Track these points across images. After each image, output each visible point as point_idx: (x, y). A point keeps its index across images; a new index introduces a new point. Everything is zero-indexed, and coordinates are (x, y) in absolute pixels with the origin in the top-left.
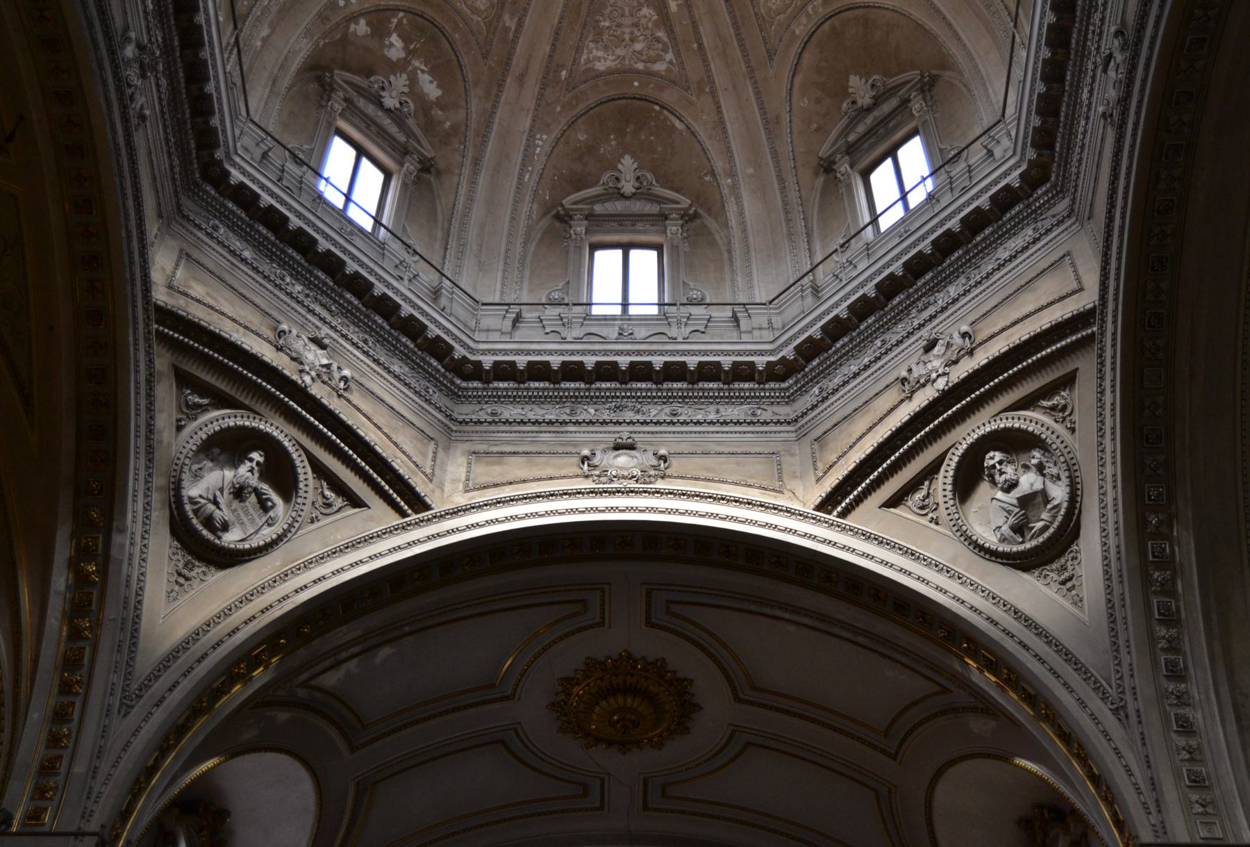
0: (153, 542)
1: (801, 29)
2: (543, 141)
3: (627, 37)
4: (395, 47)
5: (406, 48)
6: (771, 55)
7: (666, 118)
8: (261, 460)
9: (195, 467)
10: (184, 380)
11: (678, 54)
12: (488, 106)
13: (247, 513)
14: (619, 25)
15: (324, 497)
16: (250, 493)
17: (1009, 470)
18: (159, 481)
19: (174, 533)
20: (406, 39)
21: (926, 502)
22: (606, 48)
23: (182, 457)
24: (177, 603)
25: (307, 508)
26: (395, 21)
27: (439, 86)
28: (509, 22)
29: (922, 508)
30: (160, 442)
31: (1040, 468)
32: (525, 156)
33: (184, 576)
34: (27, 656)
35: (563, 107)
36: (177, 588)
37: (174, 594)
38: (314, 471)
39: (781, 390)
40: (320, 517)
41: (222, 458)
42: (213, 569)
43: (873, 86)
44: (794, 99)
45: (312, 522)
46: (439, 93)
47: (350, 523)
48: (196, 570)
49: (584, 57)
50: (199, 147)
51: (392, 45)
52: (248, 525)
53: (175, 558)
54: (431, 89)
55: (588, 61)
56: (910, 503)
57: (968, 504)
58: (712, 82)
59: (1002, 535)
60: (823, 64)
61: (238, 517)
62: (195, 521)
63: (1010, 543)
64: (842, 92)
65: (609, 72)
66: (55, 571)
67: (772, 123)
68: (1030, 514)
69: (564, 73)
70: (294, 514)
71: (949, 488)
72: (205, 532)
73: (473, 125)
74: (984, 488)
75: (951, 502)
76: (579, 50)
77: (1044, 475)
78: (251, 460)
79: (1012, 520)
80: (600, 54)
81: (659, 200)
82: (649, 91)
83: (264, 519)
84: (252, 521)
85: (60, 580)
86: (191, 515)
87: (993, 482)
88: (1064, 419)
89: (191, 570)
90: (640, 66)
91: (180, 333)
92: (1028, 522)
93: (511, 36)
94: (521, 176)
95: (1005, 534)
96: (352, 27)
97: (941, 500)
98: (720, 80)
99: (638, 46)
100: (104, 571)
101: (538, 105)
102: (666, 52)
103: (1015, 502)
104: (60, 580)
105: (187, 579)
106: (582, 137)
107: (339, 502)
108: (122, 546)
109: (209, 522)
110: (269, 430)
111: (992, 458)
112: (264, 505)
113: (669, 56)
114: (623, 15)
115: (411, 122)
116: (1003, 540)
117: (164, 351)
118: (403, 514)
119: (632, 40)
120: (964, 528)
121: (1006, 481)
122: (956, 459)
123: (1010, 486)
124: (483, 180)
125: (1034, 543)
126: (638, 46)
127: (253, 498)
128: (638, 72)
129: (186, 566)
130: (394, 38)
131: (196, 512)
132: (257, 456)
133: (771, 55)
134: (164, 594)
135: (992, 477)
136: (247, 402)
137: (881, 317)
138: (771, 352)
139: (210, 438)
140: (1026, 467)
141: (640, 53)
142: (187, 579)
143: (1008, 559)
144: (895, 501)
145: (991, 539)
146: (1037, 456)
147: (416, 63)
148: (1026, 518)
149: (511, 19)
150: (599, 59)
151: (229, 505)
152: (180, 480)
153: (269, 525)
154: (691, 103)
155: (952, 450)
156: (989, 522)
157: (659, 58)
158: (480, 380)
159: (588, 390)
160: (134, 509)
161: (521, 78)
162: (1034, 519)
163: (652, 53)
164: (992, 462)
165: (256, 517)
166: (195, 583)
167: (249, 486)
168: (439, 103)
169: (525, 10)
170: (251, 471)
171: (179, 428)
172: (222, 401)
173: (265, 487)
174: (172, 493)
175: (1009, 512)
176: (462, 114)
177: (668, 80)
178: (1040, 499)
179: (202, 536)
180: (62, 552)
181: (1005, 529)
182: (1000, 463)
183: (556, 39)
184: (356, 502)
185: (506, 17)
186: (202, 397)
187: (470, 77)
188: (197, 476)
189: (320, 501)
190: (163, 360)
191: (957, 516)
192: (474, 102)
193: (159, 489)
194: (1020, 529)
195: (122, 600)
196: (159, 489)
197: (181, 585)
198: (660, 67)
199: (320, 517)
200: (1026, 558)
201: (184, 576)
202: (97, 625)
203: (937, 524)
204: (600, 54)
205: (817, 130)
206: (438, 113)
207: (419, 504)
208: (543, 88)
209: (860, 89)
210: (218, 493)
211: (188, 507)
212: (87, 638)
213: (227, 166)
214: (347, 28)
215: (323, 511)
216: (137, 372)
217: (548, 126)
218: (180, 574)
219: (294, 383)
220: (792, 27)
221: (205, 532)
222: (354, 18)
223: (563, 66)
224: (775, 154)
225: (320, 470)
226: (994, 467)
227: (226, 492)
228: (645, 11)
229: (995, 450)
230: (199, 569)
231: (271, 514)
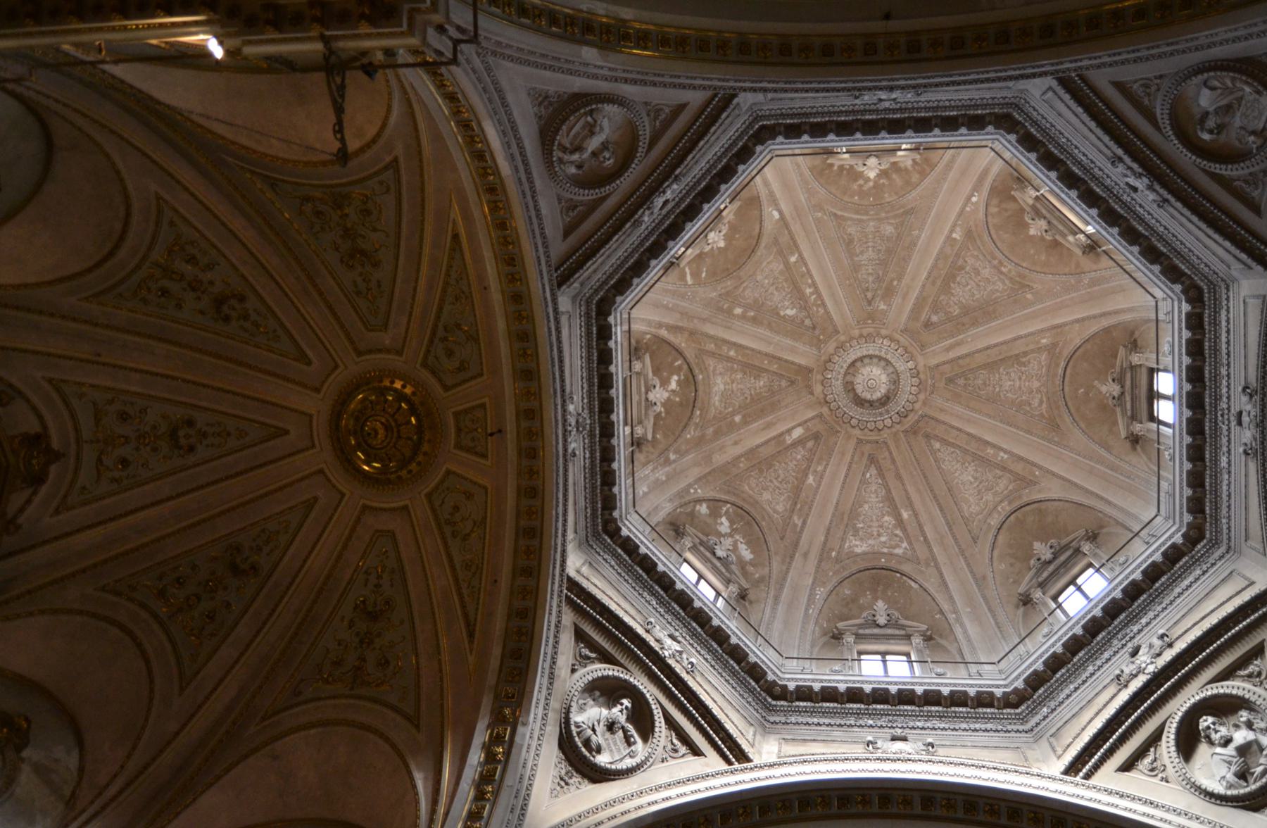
0: (544, 751)
1: (994, 521)
2: (821, 592)
3: (875, 533)
4: (724, 525)
5: (731, 526)
6: (975, 540)
7: (905, 582)
8: (629, 705)
9: (581, 702)
10: (580, 636)
11: (910, 543)
12: (784, 568)
13: (615, 744)
14: (870, 527)
15: (672, 743)
17: (1223, 731)
18: (555, 704)
19: (561, 746)
20: (732, 522)
21: (1155, 764)
22: (862, 540)
23: (573, 691)
24: (557, 800)
25: (660, 749)
26: (725, 509)
27: (751, 553)
28: (797, 520)
29: (1152, 770)
30: (559, 676)
31: (1249, 725)
32: (809, 600)
33: (564, 781)
34: (441, 809)
35: (834, 573)
36: (558, 788)
37: (555, 792)
38: (666, 724)
39: (1016, 714)
40: (669, 759)
41: (601, 700)
42: (586, 781)
43: (1051, 547)
44: (995, 564)
46: (752, 556)
47: (689, 766)
48: (574, 779)
49: (847, 544)
50: (604, 509)
51: (722, 523)
52: (616, 754)
53: (559, 766)
54: (747, 554)
55: (850, 547)
56: (1140, 767)
57: (1192, 763)
58: (934, 559)
59: (1228, 782)
60: (1012, 541)
61: (609, 745)
62: (577, 739)
63: (1236, 788)
64: (1028, 554)
65: (865, 553)
66: (471, 751)
67: (980, 581)
68: (1249, 762)
69: (834, 554)
70: (650, 750)
71: (1173, 749)
72: (583, 749)
73: (774, 577)
74: (1203, 750)
75: (1177, 760)
76: (843, 540)
77: (1254, 730)
78: (622, 704)
79: (1234, 768)
80: (857, 543)
81: (903, 627)
82: (893, 564)
83: (627, 751)
84: (619, 750)
85: (476, 757)
86: (575, 734)
87: (1211, 743)
88: (1261, 683)
89: (571, 778)
90: (885, 550)
91: (582, 601)
92: (1249, 769)
93: (798, 529)
94: (807, 610)
95: (1231, 780)
96: (698, 507)
97: (1167, 761)
98: (941, 558)
99: (883, 539)
100: (508, 754)
101: (817, 572)
102: (902, 542)
103: (1234, 753)
104: (476, 757)
105: (567, 784)
106: (847, 592)
107: (683, 750)
108: (524, 735)
109: (587, 743)
110: (636, 683)
111: (1206, 721)
112: (628, 741)
113: (905, 545)
114: (872, 521)
115: (733, 567)
116: (1230, 786)
117: (569, 611)
118: (729, 763)
119: (879, 535)
120: (1193, 780)
121: (1221, 737)
122: (1175, 725)
123: (1227, 742)
124: (781, 609)
125: (1259, 784)
126: (883, 539)
127: (620, 733)
128: (884, 553)
129: (567, 773)
130: (724, 520)
131: (579, 733)
132: (626, 702)
133: (975, 540)
134: (548, 791)
135: (1208, 737)
136: (622, 661)
137: (1089, 650)
138: (1005, 686)
139: (594, 680)
140: (1237, 726)
141: (885, 543)
142: (567, 784)
143: (1238, 802)
144: (1127, 767)
145: (1219, 789)
146: (1244, 715)
147: (737, 537)
148: (1246, 764)
149: (799, 519)
150: (857, 546)
151: (603, 735)
152: (570, 706)
153: (631, 757)
154: (922, 572)
155: (1170, 720)
156: (1214, 776)
157: (898, 546)
158: (785, 699)
159: (867, 709)
160: (536, 712)
161: (806, 555)
162: (1255, 765)
163: (893, 543)
164: (1206, 724)
166: (572, 788)
167: (619, 722)
168: (752, 563)
169: (808, 515)
170: (621, 711)
171: (573, 671)
172: (606, 658)
173: (630, 727)
174: (563, 715)
175: (1230, 763)
176: (767, 570)
177: (904, 559)
178: (1255, 747)
179: (581, 752)
180: (481, 736)
181: (1230, 777)
182: (1214, 724)
183: (828, 533)
184: (696, 752)
185: (795, 518)
186: (591, 652)
187: (772, 548)
188: (582, 709)
189: (669, 747)
190: (568, 618)
191: (1184, 771)
192: (775, 565)
193: (554, 710)
194: (1243, 775)
195: (519, 776)
196: (554, 710)
197: (562, 787)
198: (899, 551)
199: (669, 759)
200: (1254, 799)
201: (564, 781)
202: (496, 793)
203: (1167, 782)
204: (857, 543)
205: (1014, 582)
206: (750, 569)
207: (742, 757)
208: (820, 561)
209: (1042, 550)
210: (596, 723)
211: (573, 727)
212: (489, 800)
213: (620, 525)
214: (695, 507)
216: (550, 614)
217: (824, 583)
218: (562, 779)
219: (656, 653)
220: (988, 521)
221: (583, 749)
222: (699, 501)
223: (833, 550)
224: (984, 597)
225: (671, 723)
226: (1208, 728)
227: (602, 724)
228: (886, 518)
229: (1207, 715)
230: (576, 779)
231: (633, 748)
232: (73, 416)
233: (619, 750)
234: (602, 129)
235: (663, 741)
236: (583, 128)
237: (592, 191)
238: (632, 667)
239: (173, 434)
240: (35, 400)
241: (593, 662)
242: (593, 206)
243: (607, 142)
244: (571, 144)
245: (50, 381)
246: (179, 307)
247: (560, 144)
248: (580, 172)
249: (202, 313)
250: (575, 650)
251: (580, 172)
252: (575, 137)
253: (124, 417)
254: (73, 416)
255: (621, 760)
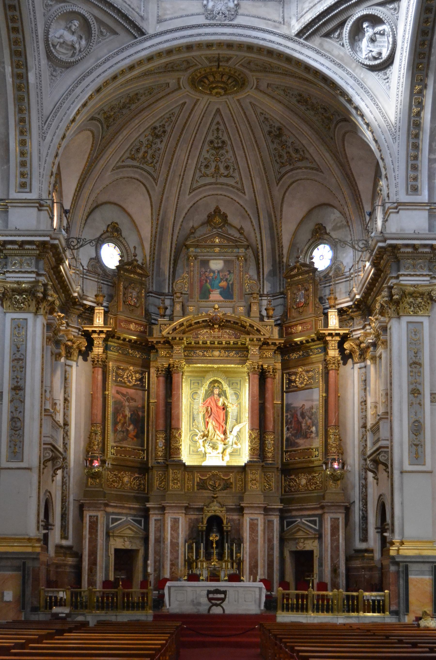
10: (327, 35)
13: (381, 42)
15: (392, 9)
16: (375, 37)
36: (387, 84)
42: (391, 67)
45: (398, 19)
48: (388, 72)
61: (380, 46)
83: (386, 37)
84: (384, 42)
105: (388, 78)
109: (375, 58)
112: (382, 34)
127: (377, 36)
151: (374, 47)
165: (384, 40)
166: (390, 77)
172: (342, 24)
186: (337, 31)
189: (392, 11)
197: (388, 82)
215: (396, 13)
218: (385, 80)
230: (388, 71)
231: (386, 33)
232: (205, 185)
233: (384, 42)
234: (61, 36)
235: (388, 13)
236: (63, 47)
237: (93, 29)
238: (349, 13)
239: (215, 148)
240: (197, 199)
241: (342, 33)
242: (100, 22)
243: (66, 27)
244: (71, 50)
245: (190, 193)
246: (159, 149)
247: (72, 56)
248: (84, 37)
249: (161, 141)
250: (333, 40)
251: (84, 37)
252: (67, 50)
253: (207, 166)
254: (205, 185)
255: (389, 42)
